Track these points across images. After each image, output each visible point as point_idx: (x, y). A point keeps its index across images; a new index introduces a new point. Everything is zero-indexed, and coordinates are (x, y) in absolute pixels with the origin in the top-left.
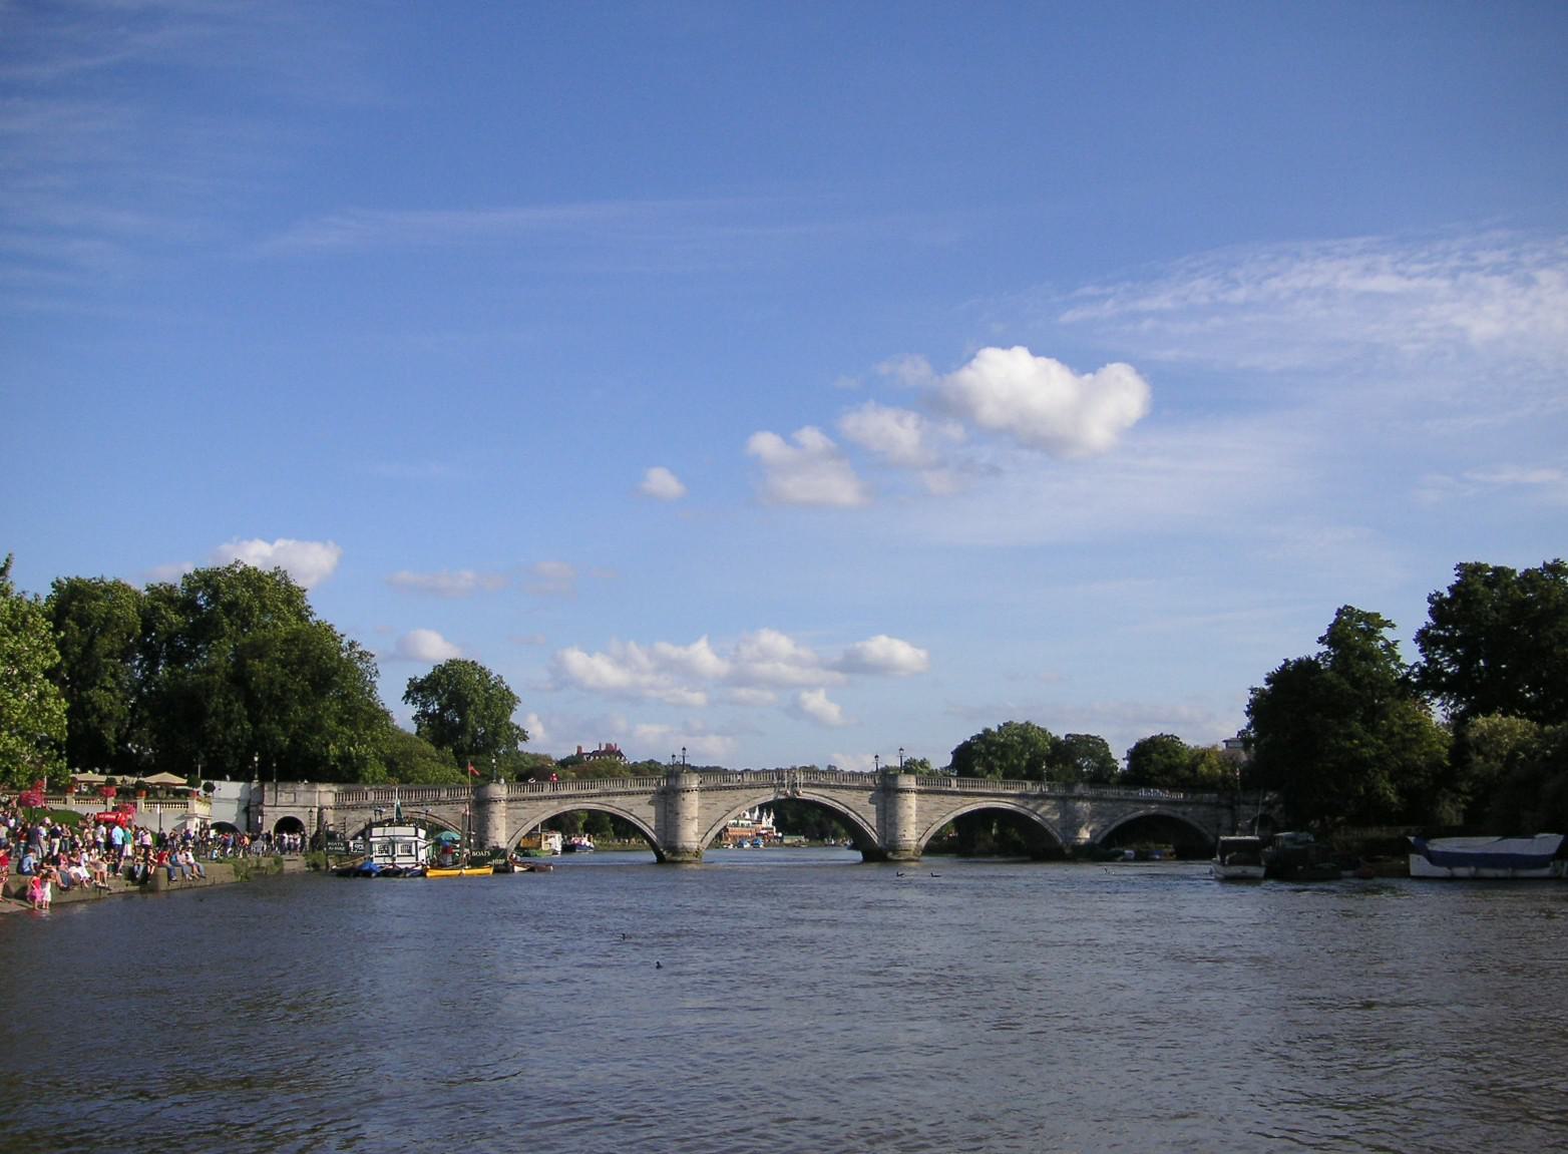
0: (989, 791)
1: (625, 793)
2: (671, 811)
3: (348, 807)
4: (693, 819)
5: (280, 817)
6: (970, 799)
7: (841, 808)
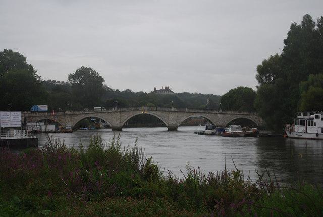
7: (156, 116)
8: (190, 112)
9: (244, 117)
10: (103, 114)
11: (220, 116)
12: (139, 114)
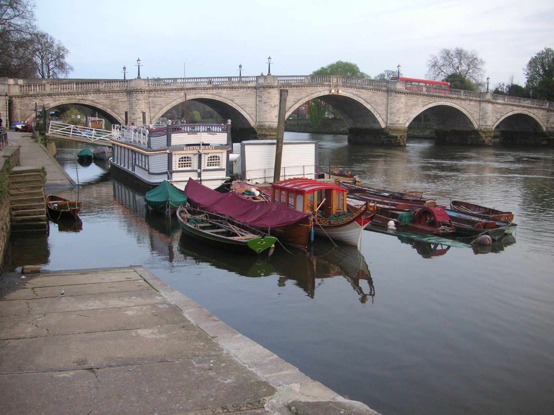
0: (442, 95)
1: (230, 88)
2: (260, 101)
3: (31, 96)
6: (432, 99)
10: (234, 92)
11: (489, 107)
12: (322, 94)
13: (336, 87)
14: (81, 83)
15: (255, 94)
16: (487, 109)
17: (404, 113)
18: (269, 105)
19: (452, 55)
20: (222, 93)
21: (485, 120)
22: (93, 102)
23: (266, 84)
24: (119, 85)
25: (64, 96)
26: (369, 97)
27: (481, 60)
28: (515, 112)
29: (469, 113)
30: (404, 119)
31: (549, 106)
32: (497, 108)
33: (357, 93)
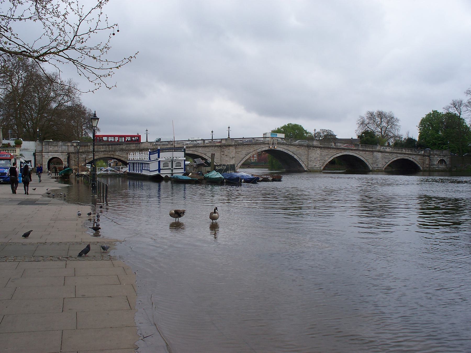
2: (224, 155)
4: (233, 158)
5: (51, 157)
6: (339, 151)
7: (291, 154)
8: (338, 149)
9: (406, 157)
11: (379, 155)
12: (264, 149)
13: (273, 145)
14: (112, 145)
15: (220, 150)
16: (378, 157)
17: (319, 160)
18: (229, 157)
19: (375, 116)
20: (199, 150)
21: (377, 163)
22: (120, 156)
23: (227, 144)
24: (134, 146)
25: (101, 153)
26: (295, 151)
27: (397, 119)
28: (399, 158)
29: (366, 160)
30: (319, 164)
31: (424, 152)
32: (386, 156)
33: (287, 148)
